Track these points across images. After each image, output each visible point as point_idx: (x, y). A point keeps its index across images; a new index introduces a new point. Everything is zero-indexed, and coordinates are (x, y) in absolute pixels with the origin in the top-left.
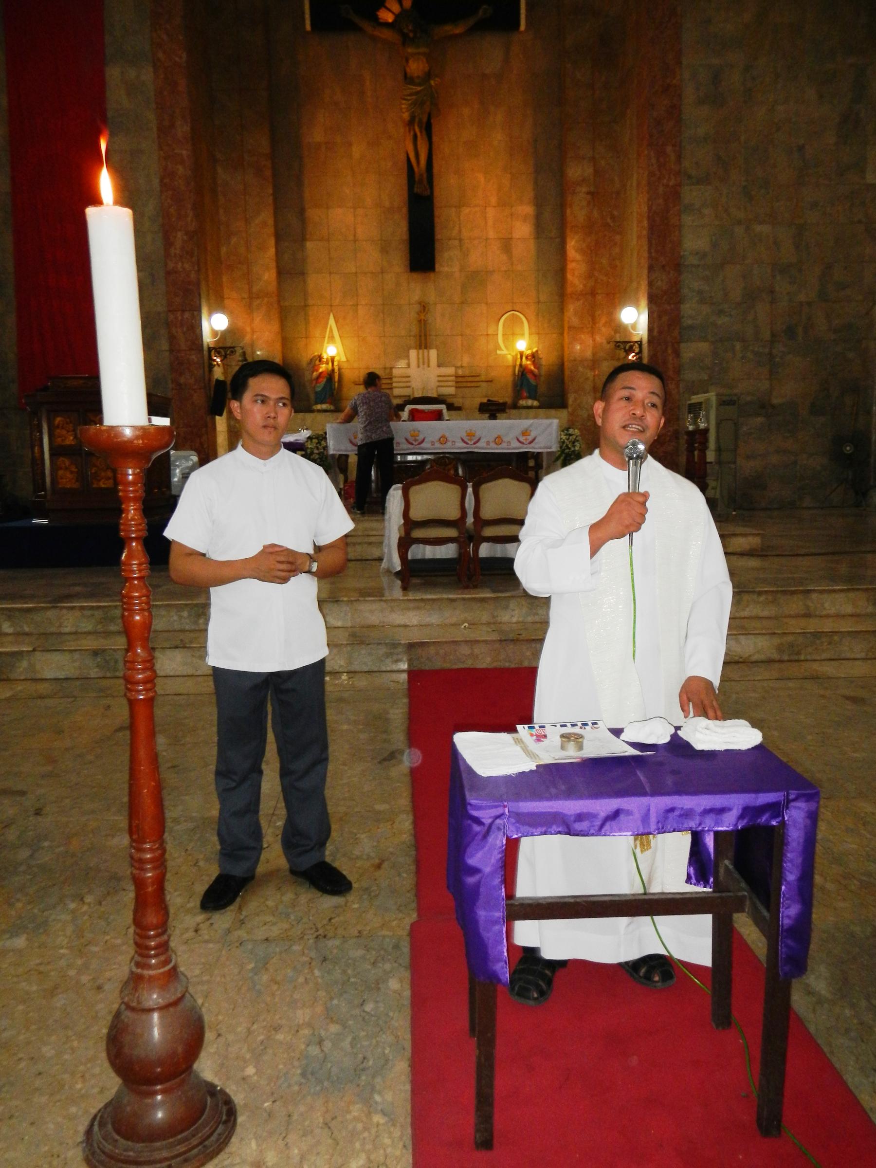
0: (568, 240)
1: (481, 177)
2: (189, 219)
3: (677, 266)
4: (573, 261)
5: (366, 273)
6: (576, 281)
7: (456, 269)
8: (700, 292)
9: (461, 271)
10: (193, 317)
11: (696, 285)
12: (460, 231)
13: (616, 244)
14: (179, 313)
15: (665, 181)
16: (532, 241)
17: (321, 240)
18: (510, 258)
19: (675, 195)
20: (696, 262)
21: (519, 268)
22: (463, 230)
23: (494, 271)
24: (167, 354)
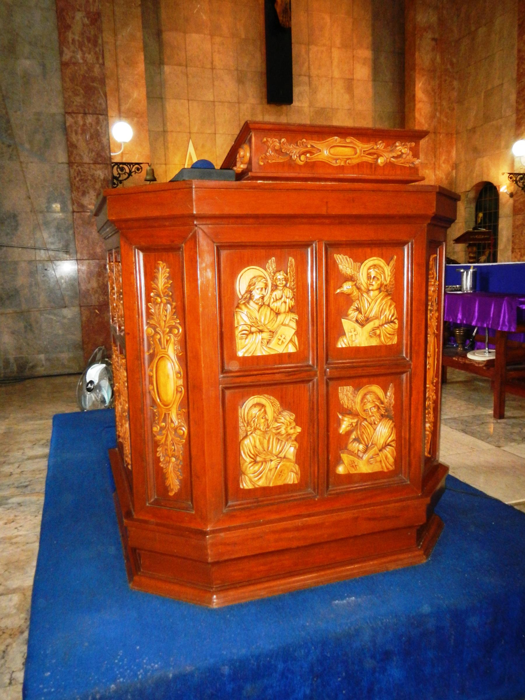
0: (417, 82)
1: (327, 18)
4: (419, 102)
5: (222, 102)
6: (423, 121)
7: (306, 105)
9: (311, 105)
10: (98, 122)
12: (309, 68)
13: (454, 88)
14: (80, 117)
16: (370, 84)
17: (180, 65)
18: (352, 97)
21: (359, 107)
22: (312, 67)
23: (338, 109)
24: (66, 166)
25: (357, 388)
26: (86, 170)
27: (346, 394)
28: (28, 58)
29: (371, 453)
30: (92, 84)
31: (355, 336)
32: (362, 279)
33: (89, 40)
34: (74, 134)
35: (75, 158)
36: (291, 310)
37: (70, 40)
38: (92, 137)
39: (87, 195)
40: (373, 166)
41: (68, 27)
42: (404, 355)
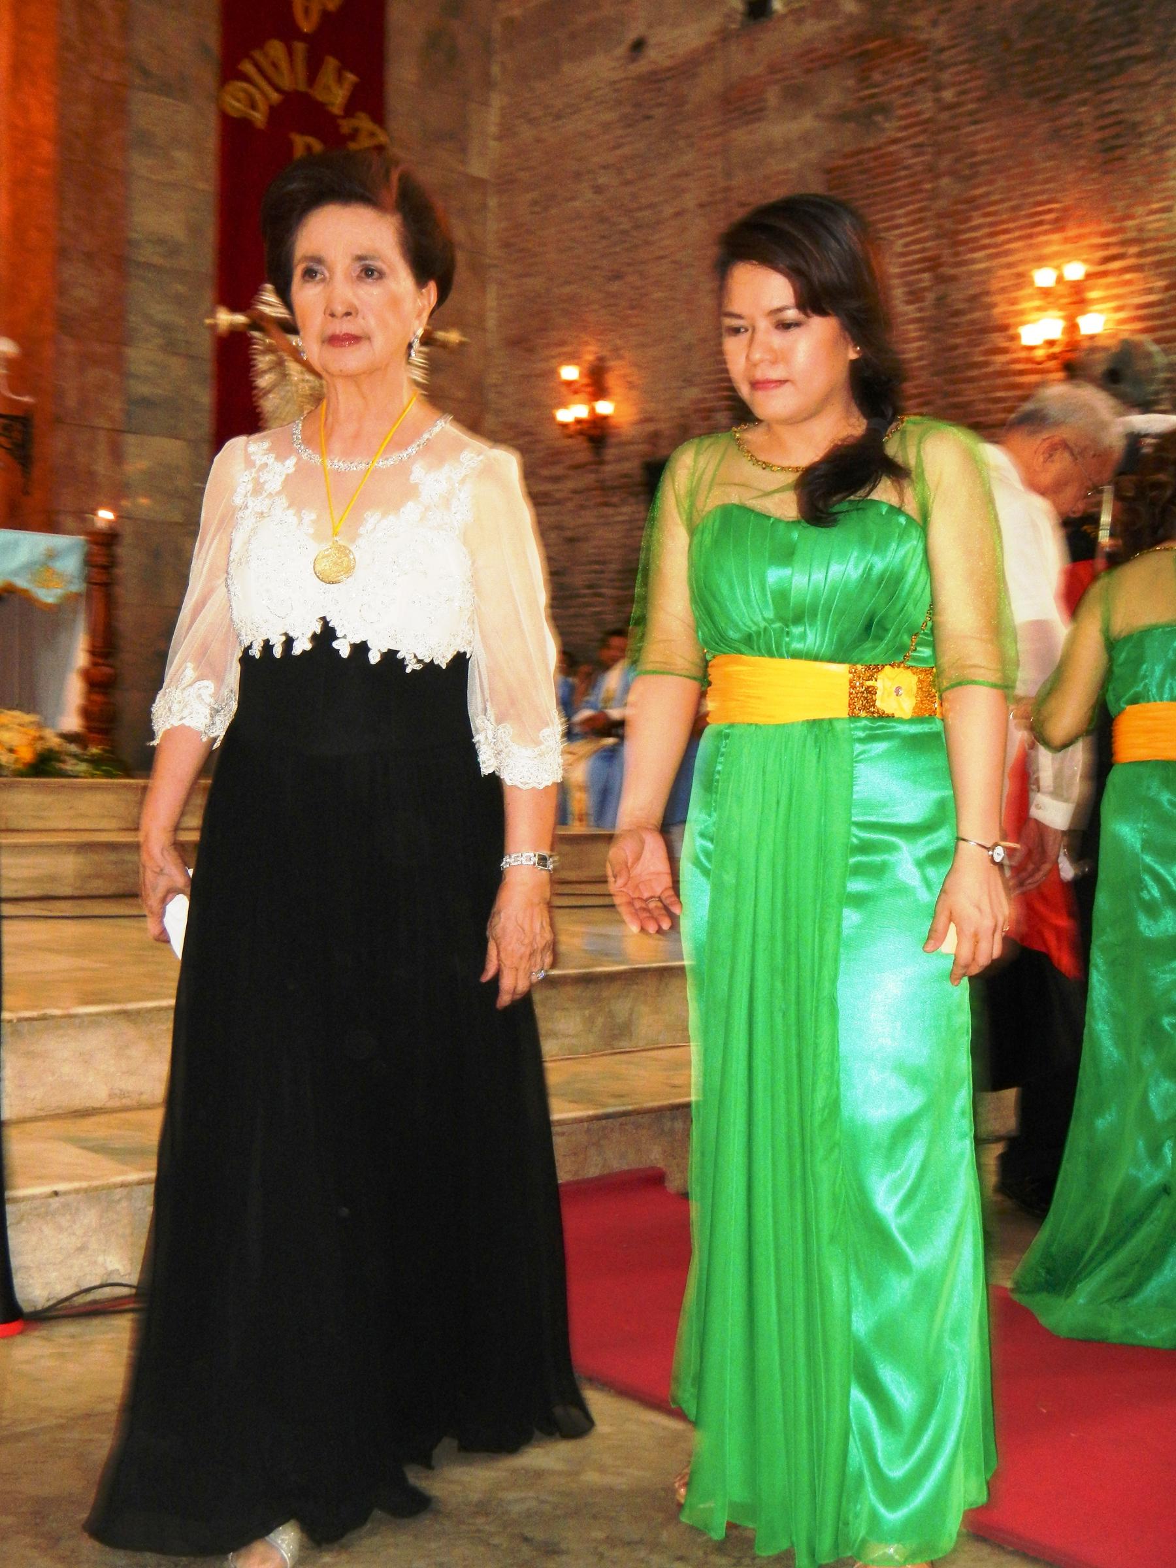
3: (117, 258)
8: (166, 328)
11: (160, 311)
15: (94, 68)
19: (112, 104)
20: (157, 260)
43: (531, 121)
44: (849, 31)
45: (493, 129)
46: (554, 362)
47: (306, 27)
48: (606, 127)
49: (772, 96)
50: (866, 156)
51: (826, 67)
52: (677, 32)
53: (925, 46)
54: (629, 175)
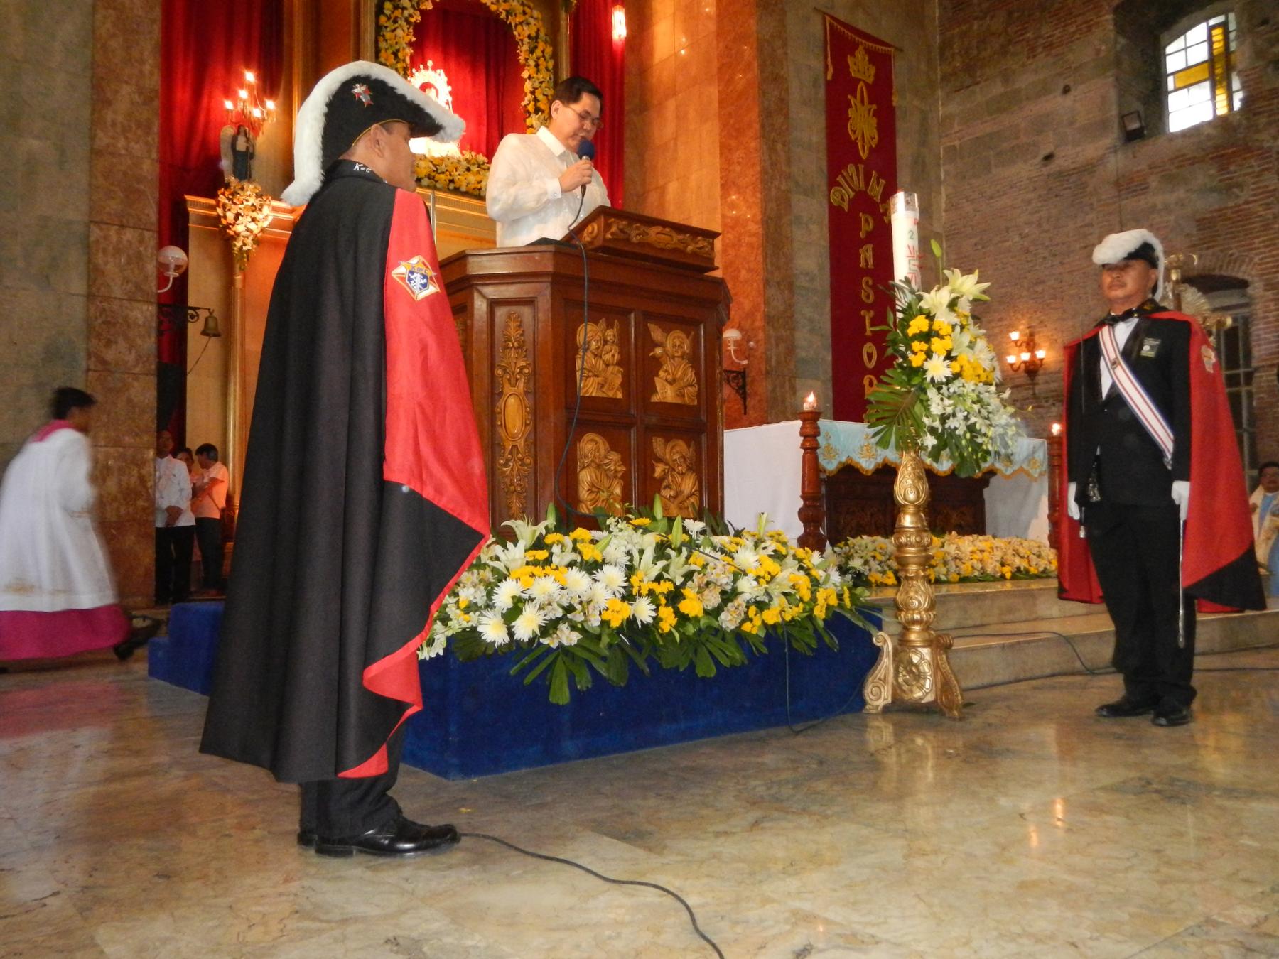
2: (147, 68)
3: (788, 284)
8: (811, 320)
11: (808, 311)
14: (113, 232)
15: (777, 183)
19: (784, 203)
20: (807, 285)
25: (667, 441)
26: (115, 308)
27: (658, 445)
28: (37, 137)
29: (680, 498)
30: (136, 186)
31: (665, 393)
32: (669, 347)
33: (139, 125)
34: (100, 255)
35: (99, 289)
36: (619, 364)
37: (109, 120)
38: (129, 263)
39: (114, 346)
40: (683, 252)
41: (108, 103)
42: (704, 418)
43: (972, 201)
44: (1209, 144)
45: (943, 206)
46: (996, 331)
47: (864, 155)
48: (1029, 202)
49: (1154, 182)
50: (1229, 212)
51: (1192, 164)
52: (1079, 149)
53: (1270, 148)
54: (1046, 227)
